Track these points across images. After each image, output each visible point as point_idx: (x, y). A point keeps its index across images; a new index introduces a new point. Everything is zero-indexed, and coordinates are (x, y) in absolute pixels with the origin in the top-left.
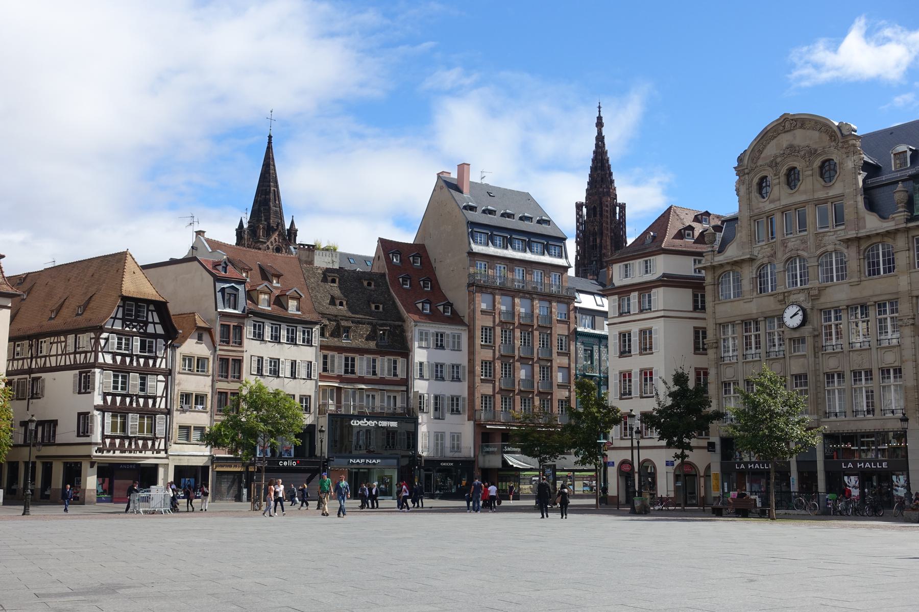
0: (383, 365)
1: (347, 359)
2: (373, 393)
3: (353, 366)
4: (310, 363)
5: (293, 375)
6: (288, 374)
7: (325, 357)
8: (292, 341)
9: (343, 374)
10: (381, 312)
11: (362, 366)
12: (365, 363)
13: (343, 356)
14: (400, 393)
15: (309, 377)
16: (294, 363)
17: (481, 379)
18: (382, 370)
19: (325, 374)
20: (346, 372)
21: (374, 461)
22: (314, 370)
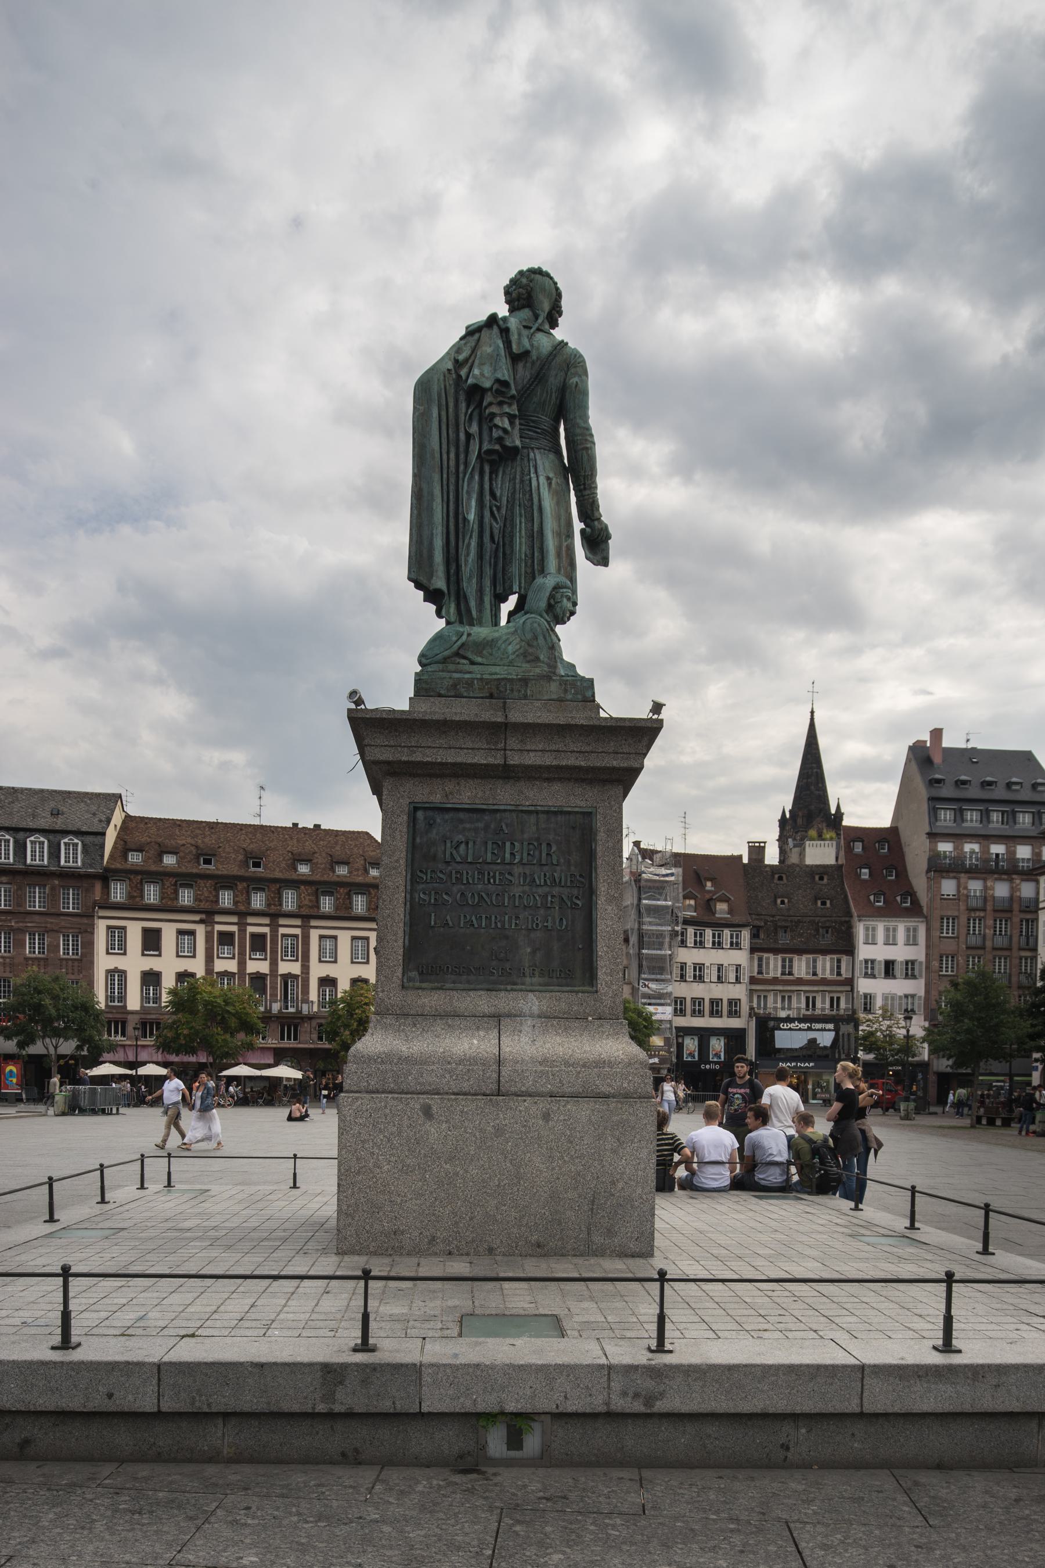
0: (825, 965)
1: (784, 960)
2: (814, 995)
3: (791, 967)
4: (738, 967)
5: (720, 980)
6: (715, 979)
7: (760, 959)
8: (718, 945)
9: (779, 975)
10: (828, 909)
11: (801, 967)
12: (804, 964)
13: (779, 957)
14: (820, 994)
15: (738, 980)
16: (720, 967)
17: (940, 975)
18: (824, 970)
19: (760, 976)
20: (783, 973)
21: (807, 1064)
22: (744, 974)
